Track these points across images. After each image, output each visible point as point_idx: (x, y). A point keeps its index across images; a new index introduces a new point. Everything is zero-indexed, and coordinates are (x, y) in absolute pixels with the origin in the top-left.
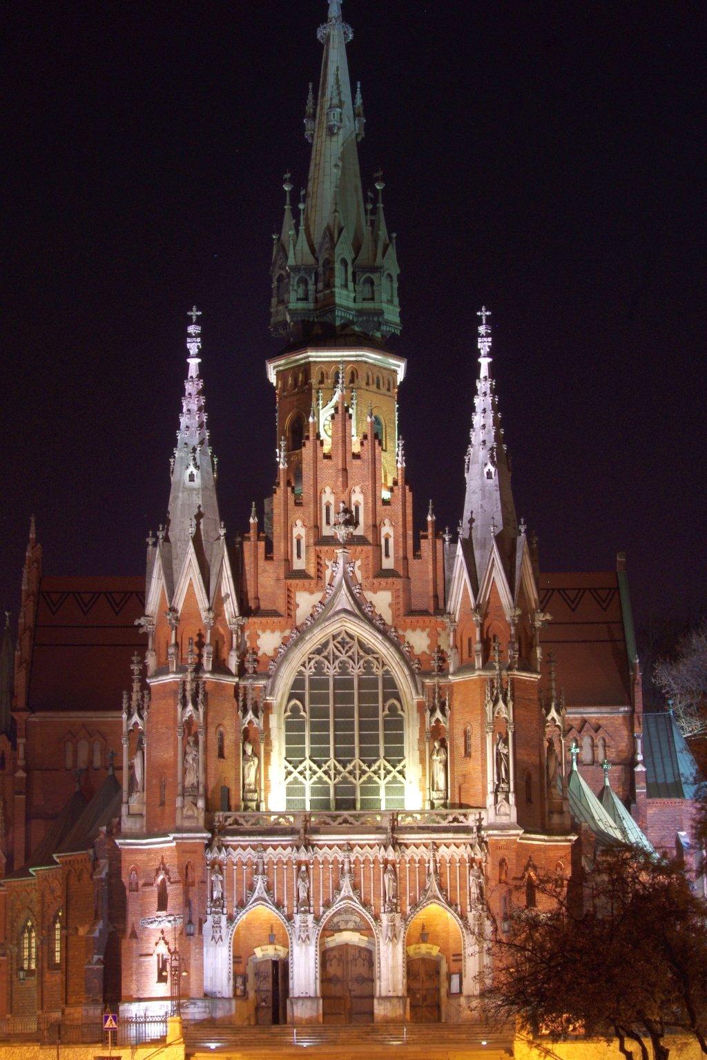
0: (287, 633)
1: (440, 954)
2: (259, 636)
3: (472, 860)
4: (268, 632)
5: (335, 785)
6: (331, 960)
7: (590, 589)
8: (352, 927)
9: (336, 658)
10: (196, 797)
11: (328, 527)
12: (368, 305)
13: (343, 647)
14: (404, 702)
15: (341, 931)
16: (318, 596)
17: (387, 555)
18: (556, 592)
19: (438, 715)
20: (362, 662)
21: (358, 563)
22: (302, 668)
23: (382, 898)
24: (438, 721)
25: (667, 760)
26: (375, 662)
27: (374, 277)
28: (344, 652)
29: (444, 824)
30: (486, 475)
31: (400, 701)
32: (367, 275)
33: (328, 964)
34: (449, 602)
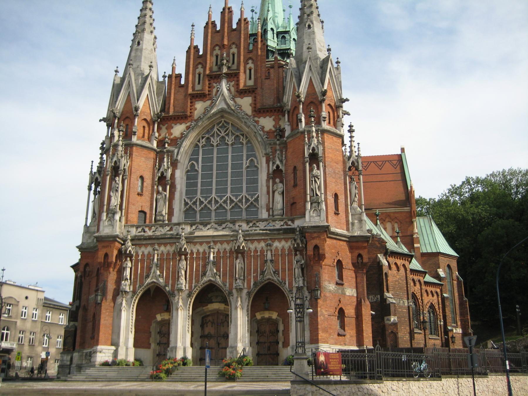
0: (188, 124)
1: (278, 318)
2: (172, 128)
3: (296, 250)
4: (178, 124)
5: (215, 210)
6: (207, 323)
7: (388, 161)
8: (220, 300)
9: (219, 135)
10: (114, 213)
11: (216, 67)
12: (283, 47)
13: (223, 130)
14: (258, 158)
15: (212, 302)
16: (209, 102)
17: (250, 78)
18: (372, 163)
19: (278, 162)
20: (233, 137)
21: (233, 83)
22: (198, 143)
23: (234, 278)
24: (278, 167)
25: (430, 238)
26: (241, 137)
27: (287, 36)
28: (222, 132)
29: (278, 227)
30: (307, 26)
31: (257, 160)
32: (283, 35)
33: (205, 325)
34: (285, 96)
